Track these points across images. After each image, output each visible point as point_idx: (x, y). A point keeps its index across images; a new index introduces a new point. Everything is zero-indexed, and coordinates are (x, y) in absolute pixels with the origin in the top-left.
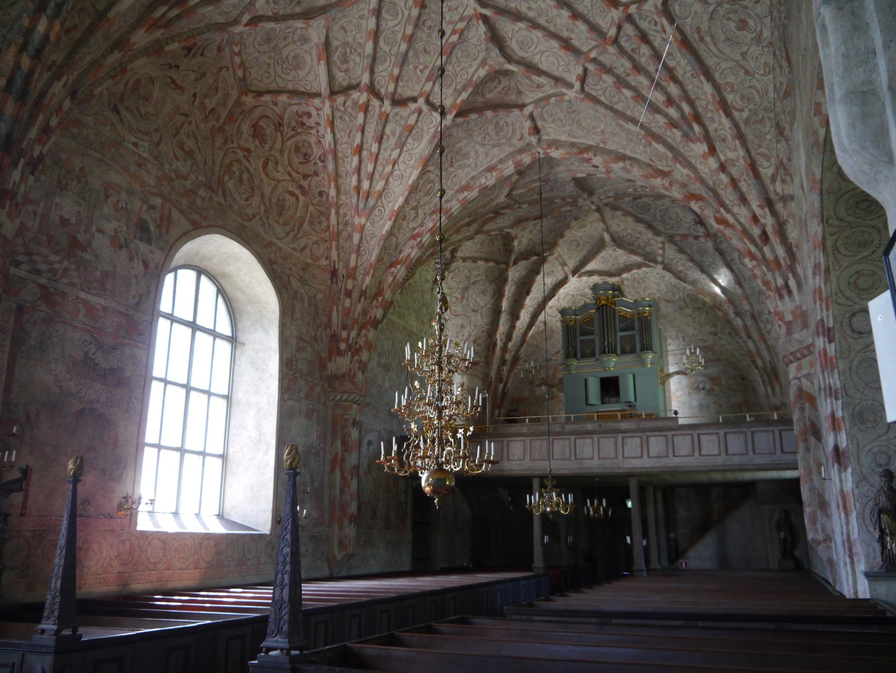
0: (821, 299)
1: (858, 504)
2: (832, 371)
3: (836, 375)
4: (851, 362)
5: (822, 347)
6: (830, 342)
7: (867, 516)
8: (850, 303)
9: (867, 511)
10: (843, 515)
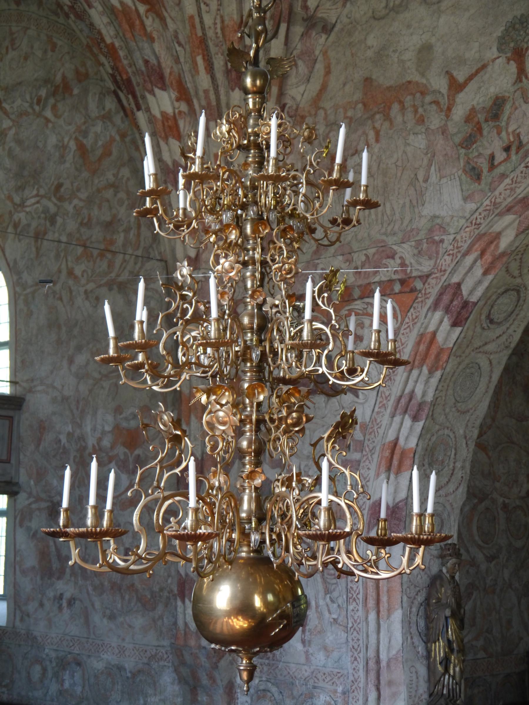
0: (483, 253)
1: (405, 598)
2: (431, 372)
3: (434, 381)
4: (459, 364)
5: (431, 328)
6: (454, 324)
7: (414, 619)
8: (516, 273)
9: (414, 610)
10: (372, 616)
